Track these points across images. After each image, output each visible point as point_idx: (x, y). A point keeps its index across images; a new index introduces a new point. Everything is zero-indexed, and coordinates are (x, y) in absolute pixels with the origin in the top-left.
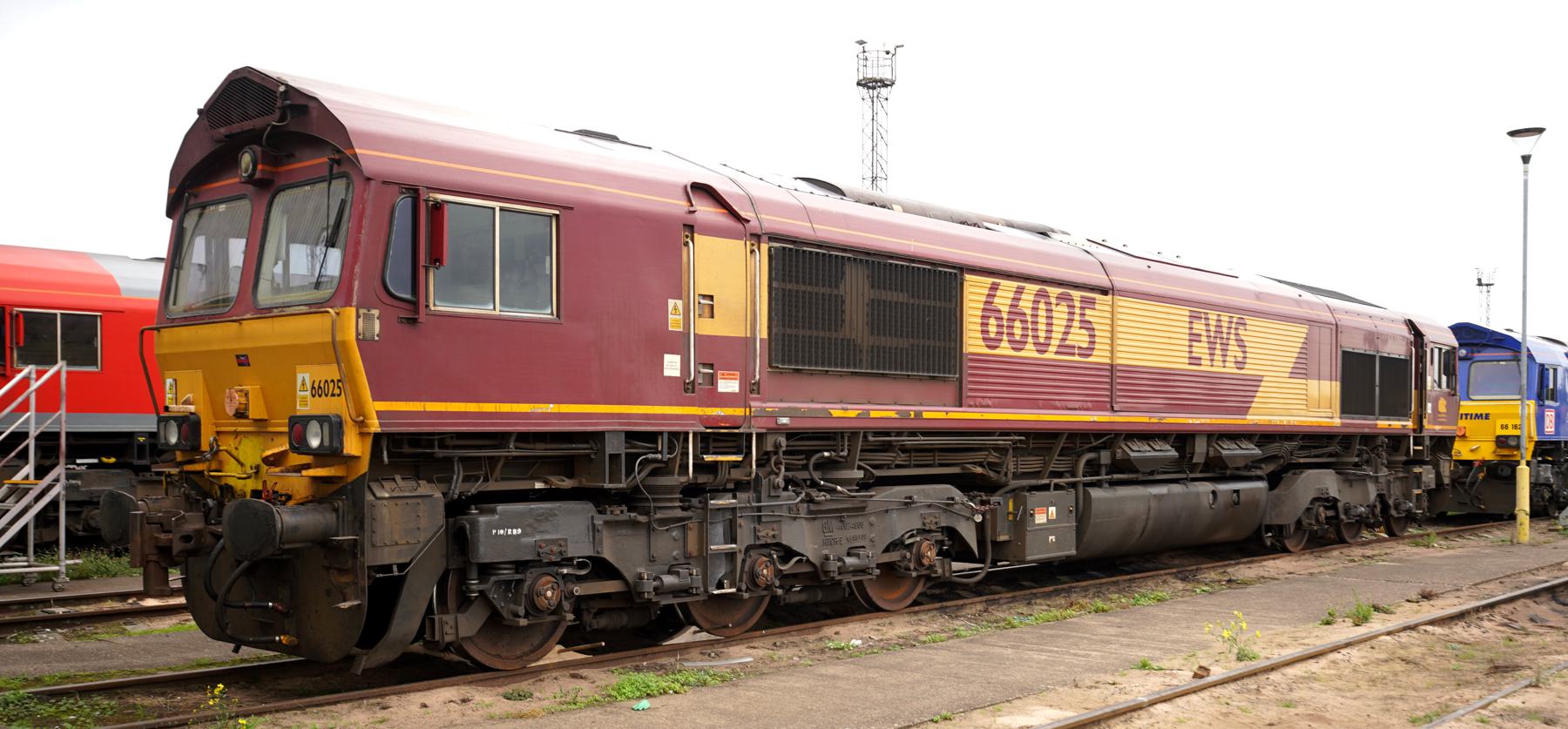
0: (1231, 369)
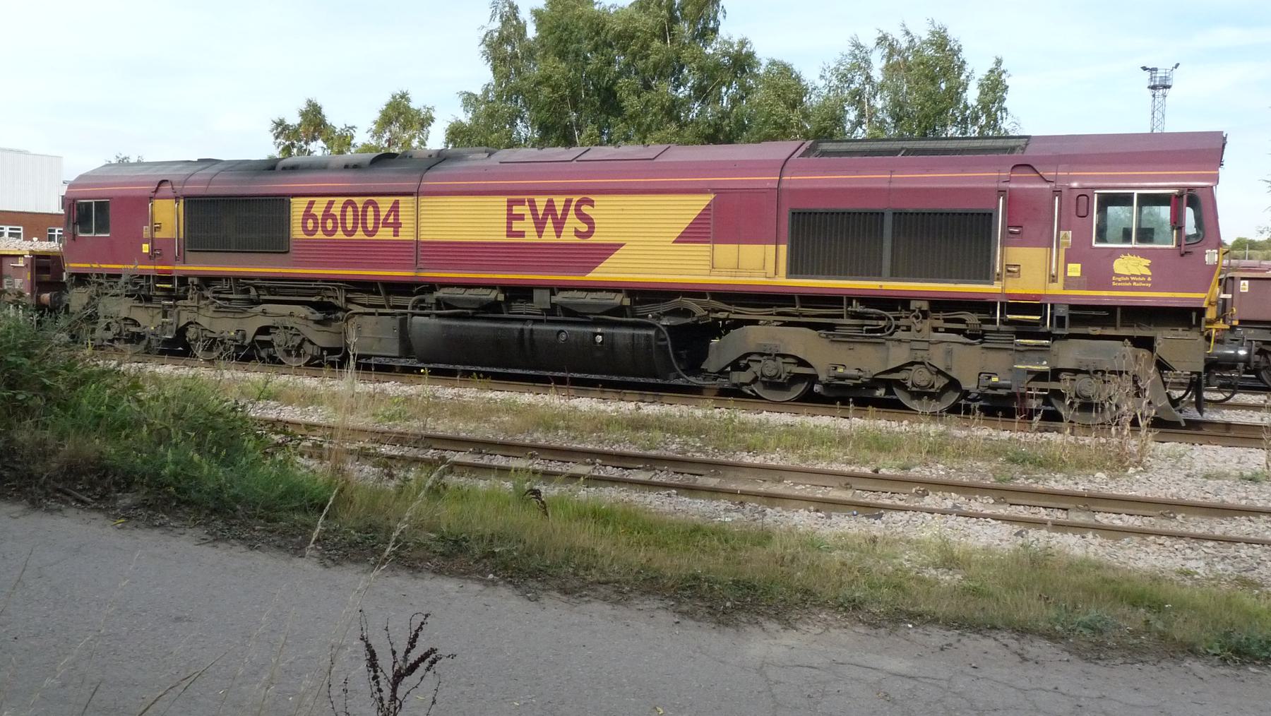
0: (568, 236)
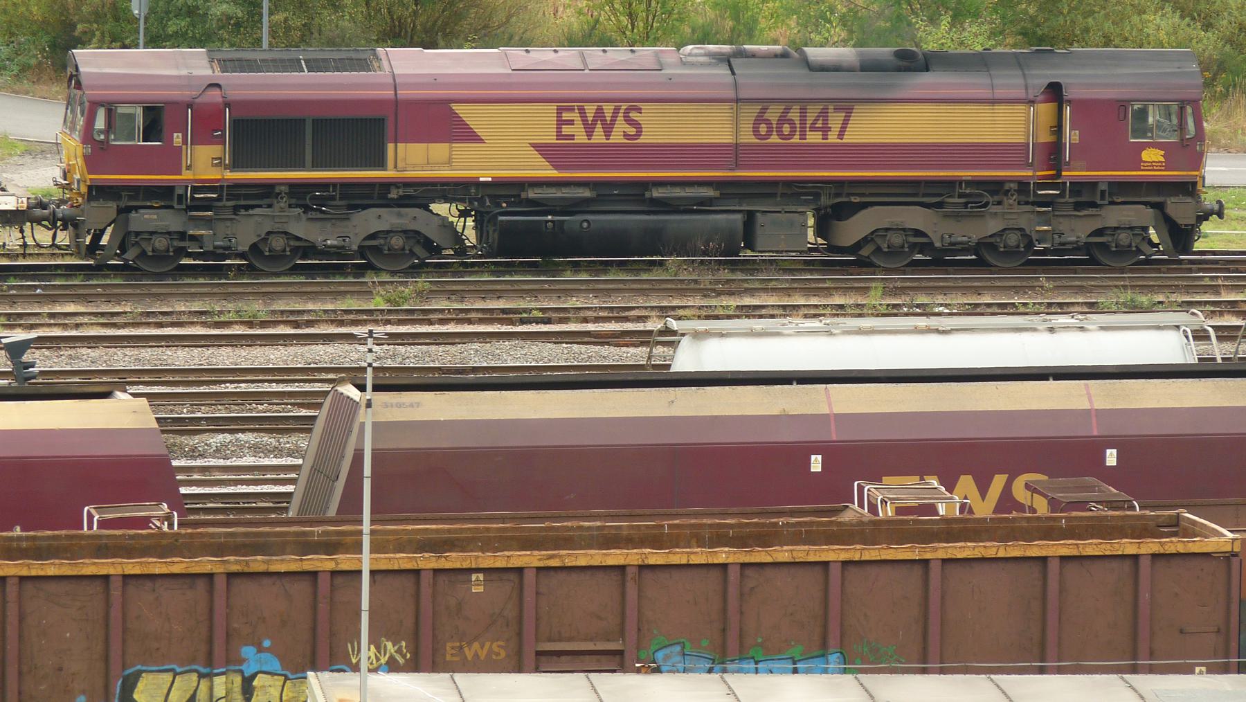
0: (617, 137)
